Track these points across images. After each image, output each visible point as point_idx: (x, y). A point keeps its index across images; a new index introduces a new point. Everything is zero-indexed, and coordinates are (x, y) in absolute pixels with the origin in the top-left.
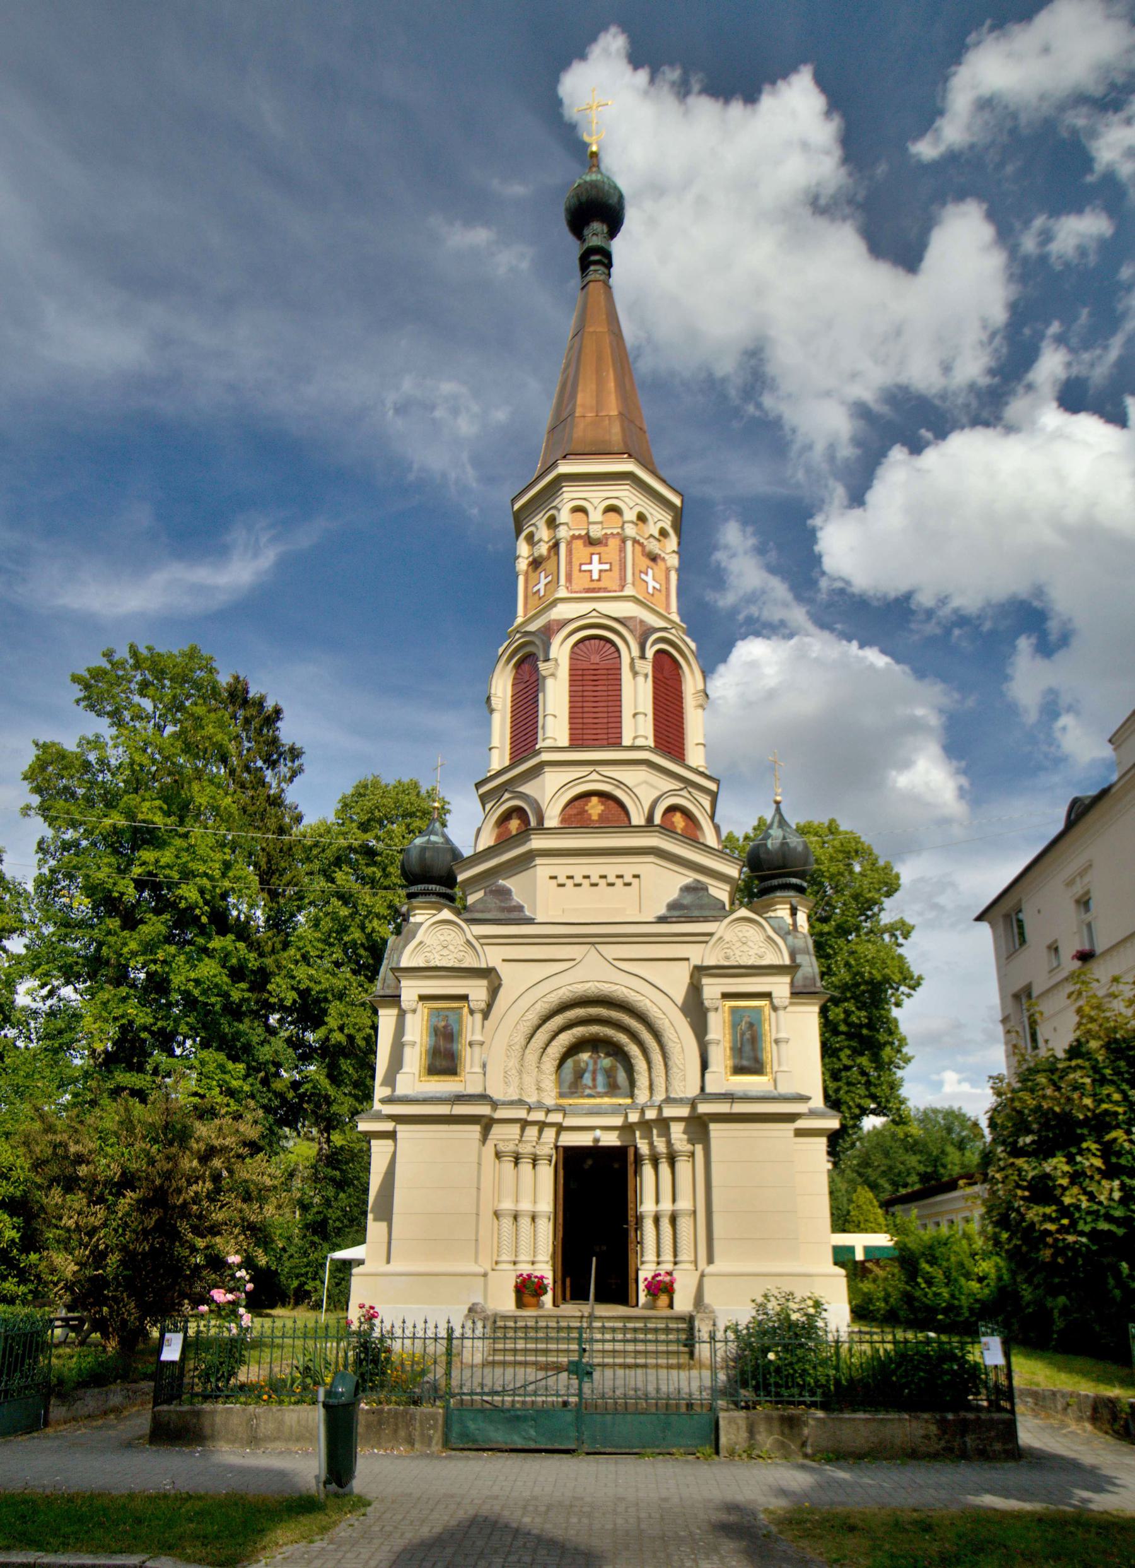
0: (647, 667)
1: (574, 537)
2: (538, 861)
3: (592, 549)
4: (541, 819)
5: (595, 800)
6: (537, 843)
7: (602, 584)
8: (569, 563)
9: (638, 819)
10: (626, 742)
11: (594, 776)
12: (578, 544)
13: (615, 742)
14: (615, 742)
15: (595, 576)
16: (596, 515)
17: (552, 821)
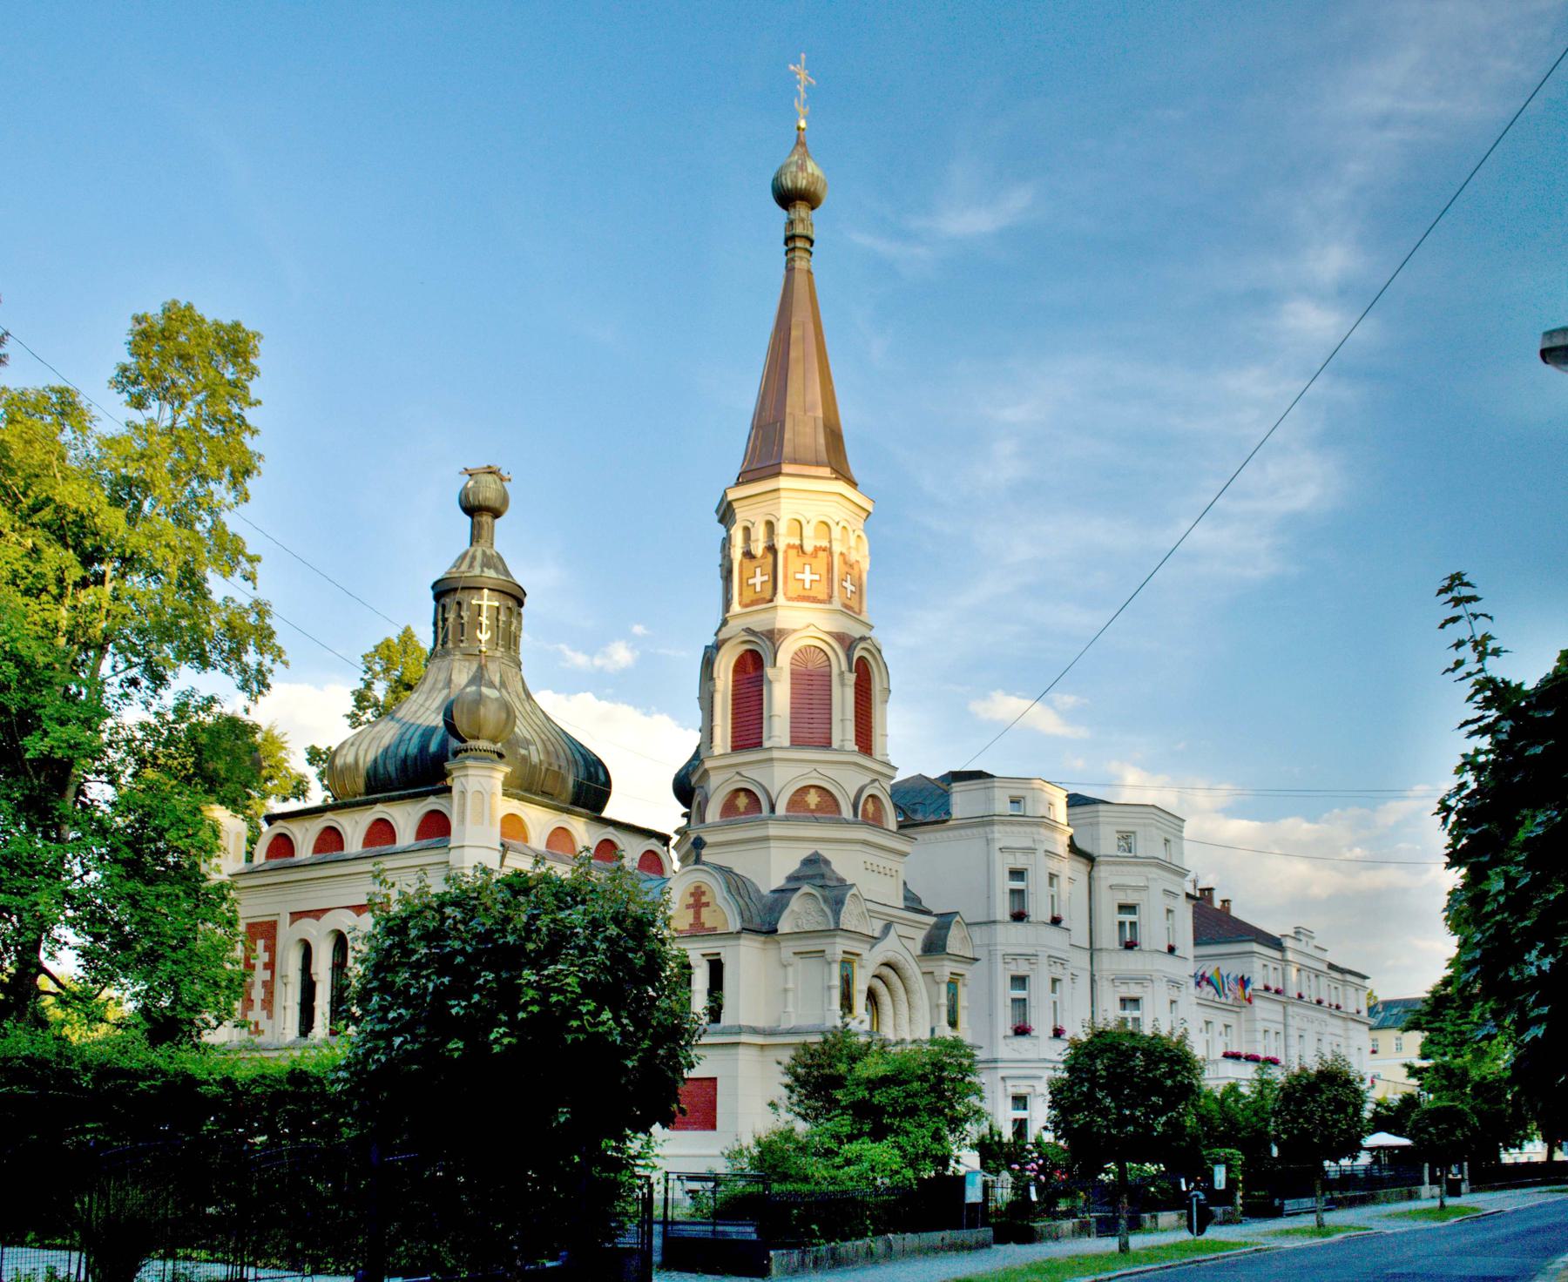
0: (851, 678)
1: (790, 546)
2: (772, 844)
3: (804, 560)
4: (773, 809)
5: (812, 791)
6: (773, 830)
7: (812, 594)
8: (785, 567)
9: (847, 812)
10: (835, 745)
11: (815, 774)
12: (793, 553)
13: (826, 744)
14: (826, 744)
15: (807, 586)
16: (808, 531)
17: (781, 810)
